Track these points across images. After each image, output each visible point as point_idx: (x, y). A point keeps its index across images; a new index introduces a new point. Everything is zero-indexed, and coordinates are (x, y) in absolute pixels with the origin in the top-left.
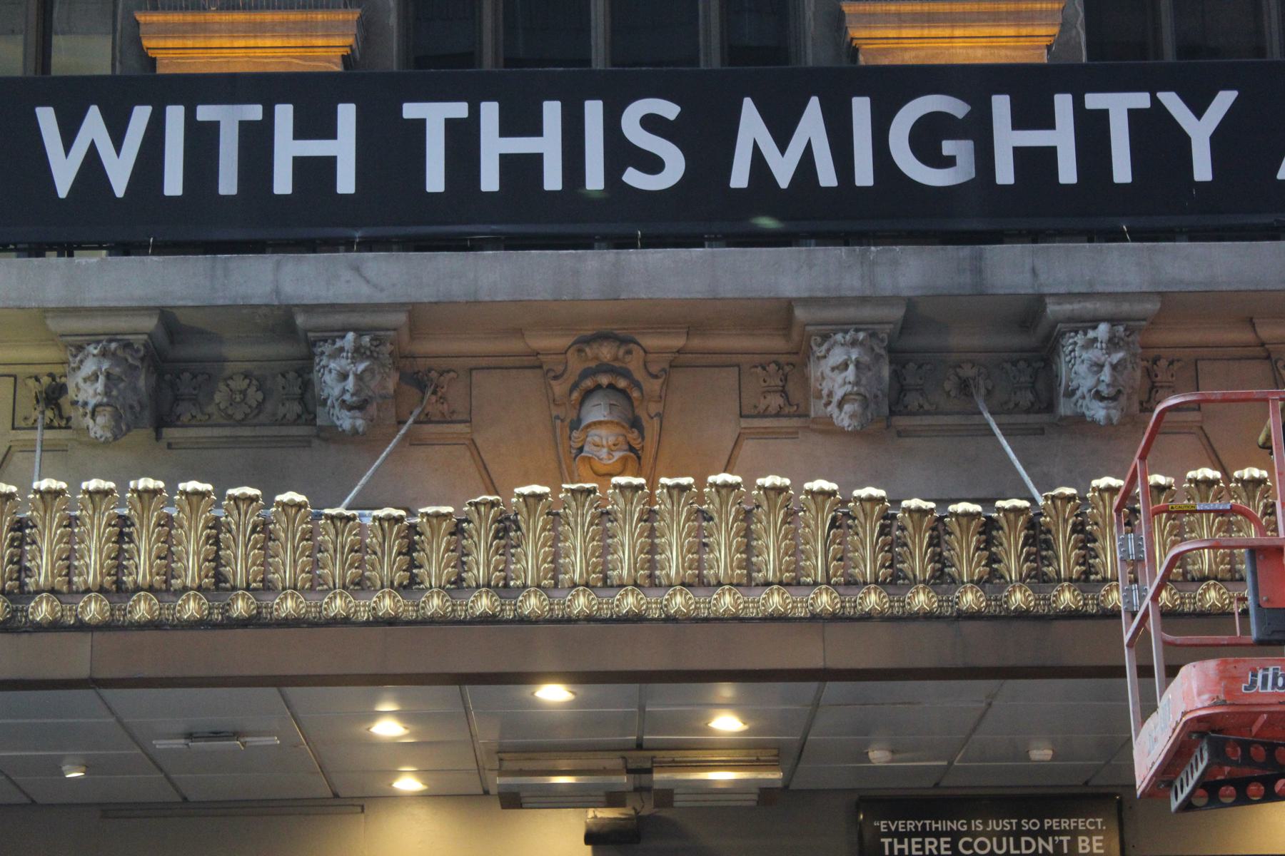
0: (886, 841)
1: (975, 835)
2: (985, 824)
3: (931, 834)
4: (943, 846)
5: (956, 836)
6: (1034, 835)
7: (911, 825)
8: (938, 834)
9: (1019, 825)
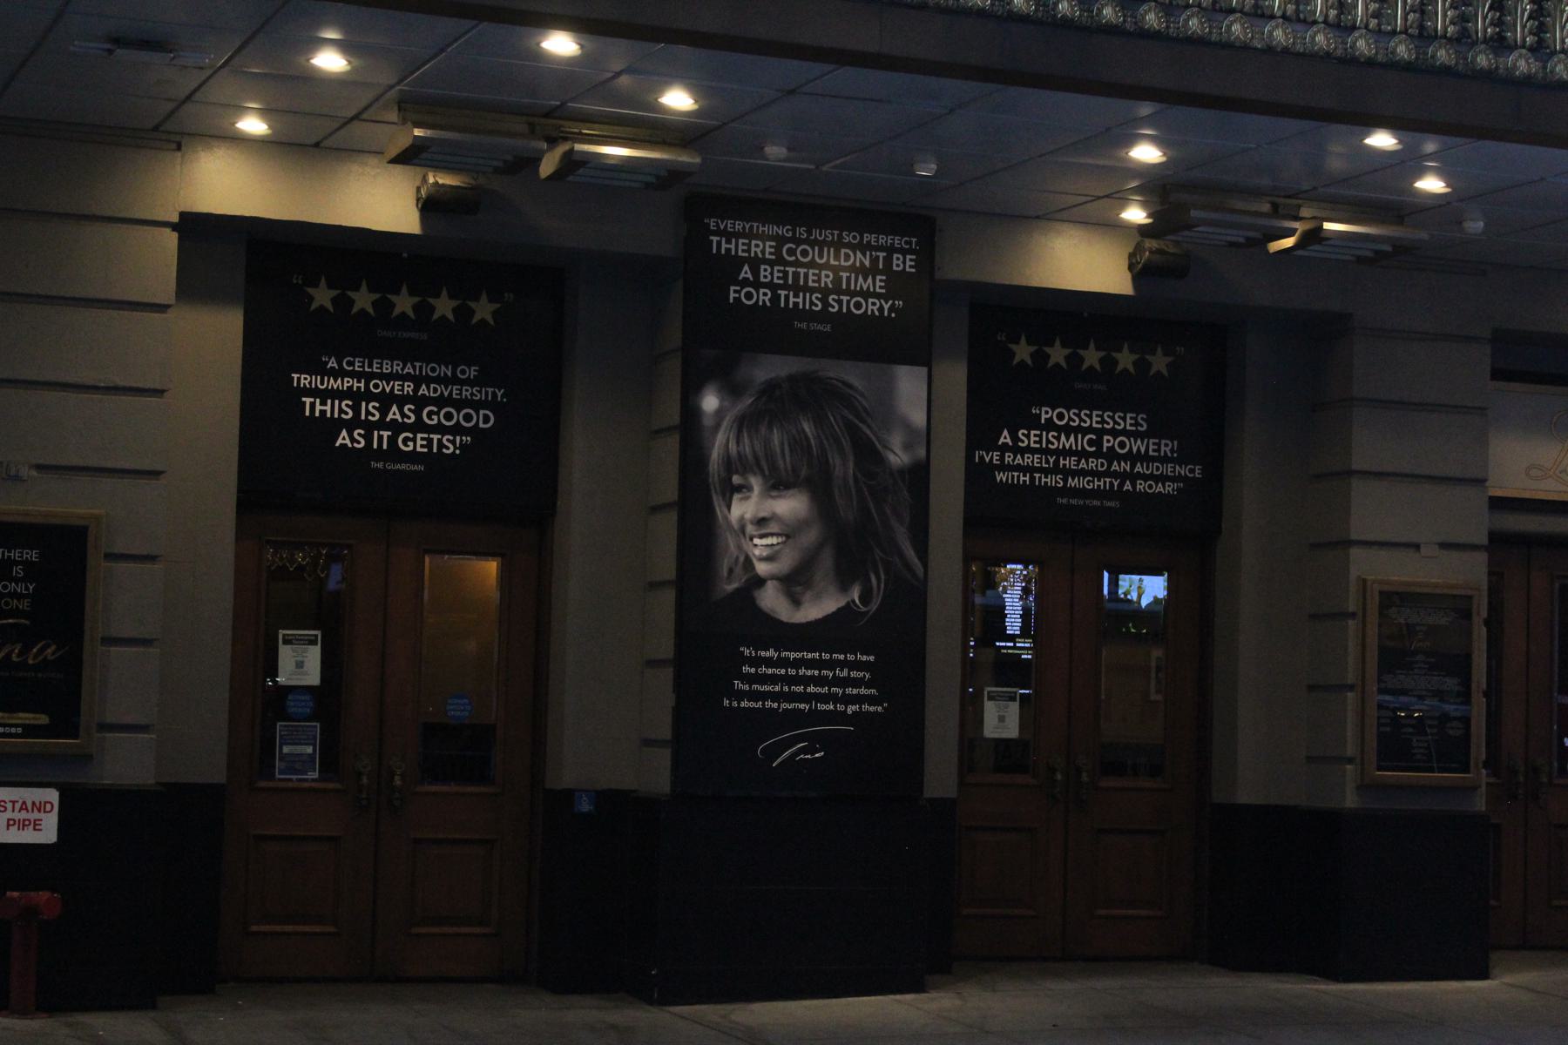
0: (715, 239)
1: (798, 242)
2: (809, 233)
3: (757, 237)
4: (768, 250)
5: (781, 241)
6: (853, 247)
7: (739, 226)
8: (763, 238)
9: (840, 236)
